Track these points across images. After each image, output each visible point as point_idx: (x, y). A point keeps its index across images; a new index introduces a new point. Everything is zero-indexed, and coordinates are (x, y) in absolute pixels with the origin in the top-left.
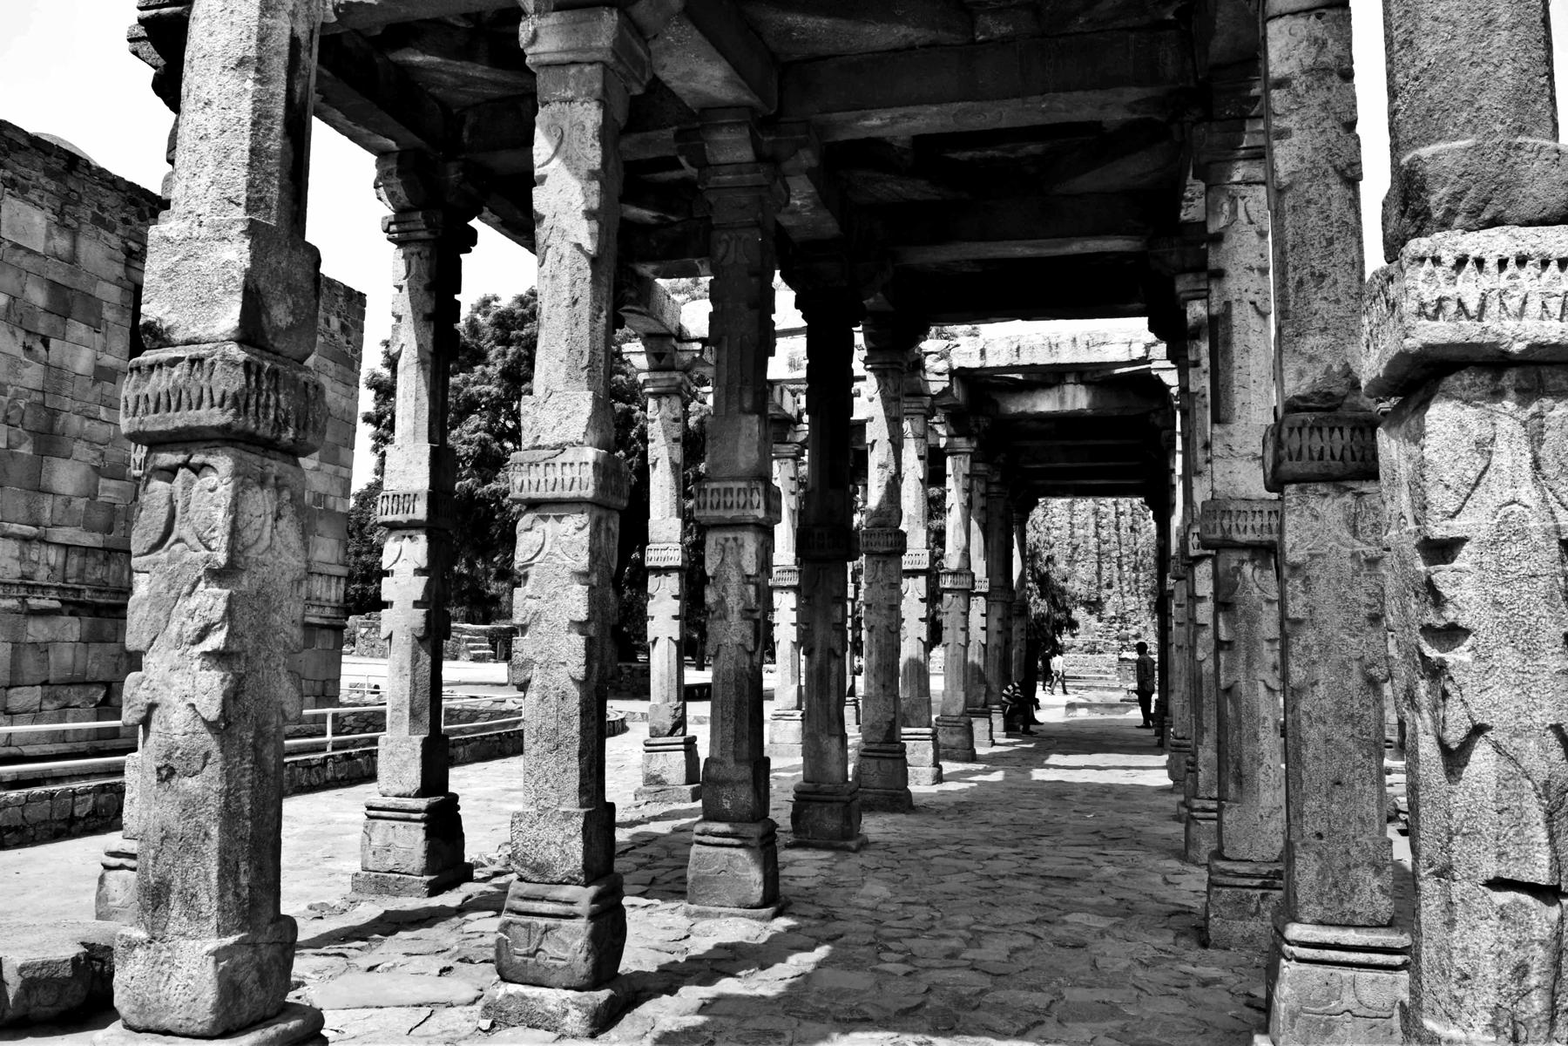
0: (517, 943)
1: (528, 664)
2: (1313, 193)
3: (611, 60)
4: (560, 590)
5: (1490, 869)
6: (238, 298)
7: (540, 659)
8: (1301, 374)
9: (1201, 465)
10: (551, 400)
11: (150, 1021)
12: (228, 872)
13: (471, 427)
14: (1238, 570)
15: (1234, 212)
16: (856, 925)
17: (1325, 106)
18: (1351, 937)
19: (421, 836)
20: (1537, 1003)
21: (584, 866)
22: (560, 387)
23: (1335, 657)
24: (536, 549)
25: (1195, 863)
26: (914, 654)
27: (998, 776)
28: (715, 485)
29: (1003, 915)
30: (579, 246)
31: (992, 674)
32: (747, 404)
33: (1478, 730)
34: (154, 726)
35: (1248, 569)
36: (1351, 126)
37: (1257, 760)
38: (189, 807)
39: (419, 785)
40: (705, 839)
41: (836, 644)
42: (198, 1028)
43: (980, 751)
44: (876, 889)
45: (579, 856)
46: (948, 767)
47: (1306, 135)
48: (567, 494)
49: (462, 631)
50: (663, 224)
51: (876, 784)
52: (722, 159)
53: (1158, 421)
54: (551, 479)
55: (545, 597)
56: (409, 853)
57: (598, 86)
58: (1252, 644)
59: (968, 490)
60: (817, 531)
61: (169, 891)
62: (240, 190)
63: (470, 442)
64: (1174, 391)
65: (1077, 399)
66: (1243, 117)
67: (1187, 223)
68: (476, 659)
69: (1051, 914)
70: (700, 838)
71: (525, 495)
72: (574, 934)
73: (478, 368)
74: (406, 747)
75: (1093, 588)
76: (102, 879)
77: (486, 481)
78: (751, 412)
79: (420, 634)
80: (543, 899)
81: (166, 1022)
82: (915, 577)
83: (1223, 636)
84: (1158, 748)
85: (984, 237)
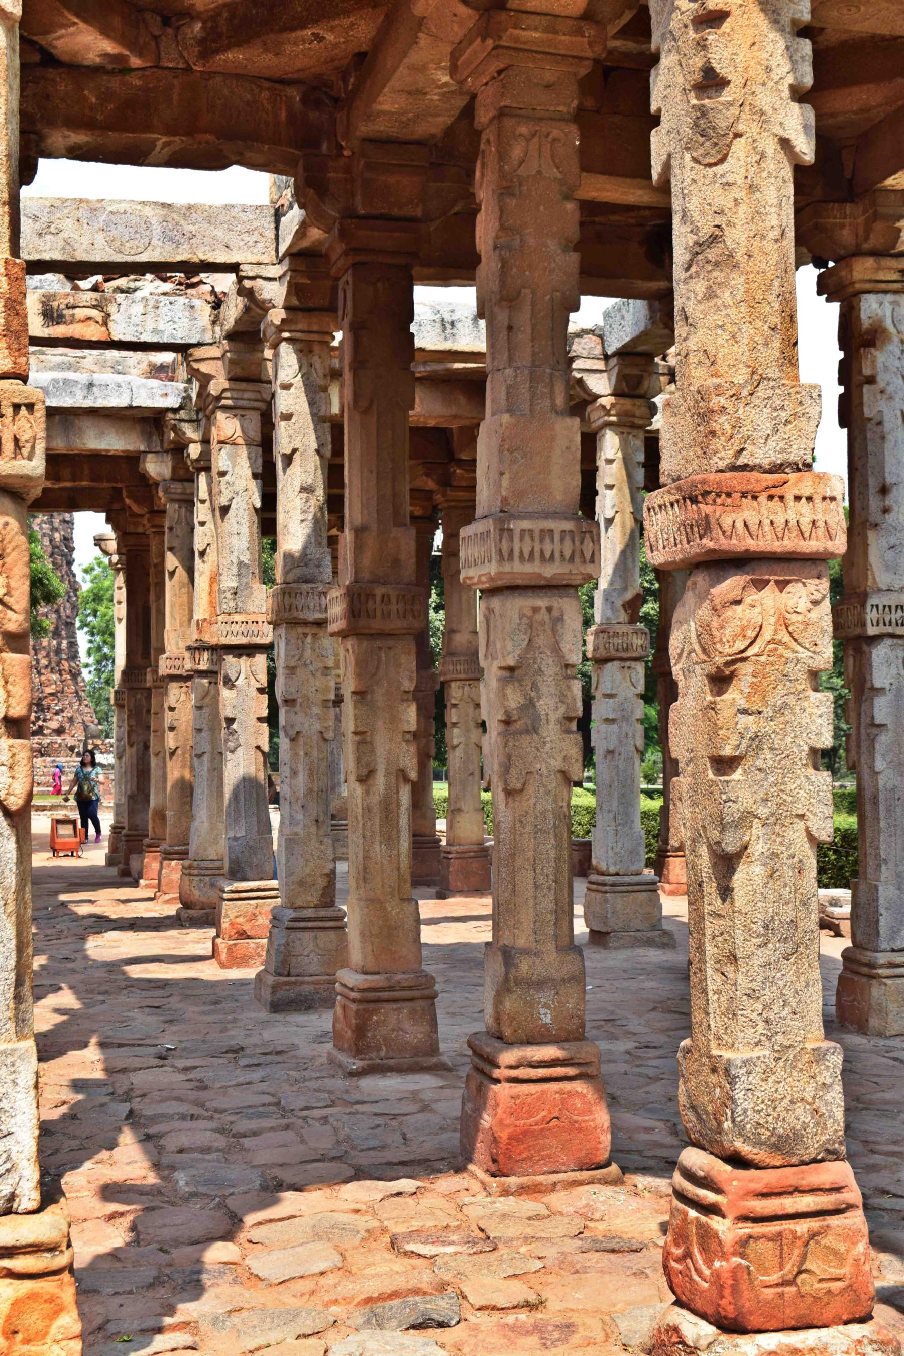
4: (791, 700)
7: (763, 811)
10: (761, 393)
21: (847, 1128)
22: (773, 372)
24: (751, 634)
25: (881, 1035)
26: (252, 771)
28: (526, 524)
30: (785, 143)
40: (522, 1073)
45: (839, 1115)
50: (116, 67)
51: (313, 969)
54: (780, 520)
55: (768, 712)
60: (379, 591)
70: (514, 1073)
80: (798, 1190)
82: (250, 655)
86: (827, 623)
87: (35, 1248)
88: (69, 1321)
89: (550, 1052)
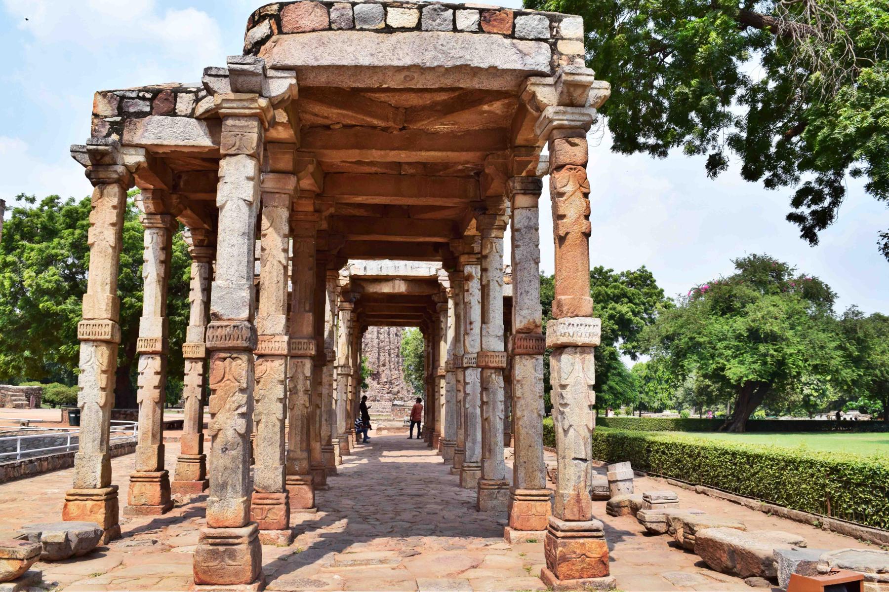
0: (257, 515)
1: (261, 413)
2: (526, 266)
3: (292, 193)
5: (573, 456)
6: (248, 307)
8: (521, 322)
9: (468, 331)
11: (220, 524)
12: (244, 479)
13: (51, 273)
14: (490, 376)
15: (492, 248)
16: (349, 513)
17: (530, 239)
18: (534, 492)
19: (159, 488)
20: (583, 484)
23: (530, 408)
27: (365, 461)
29: (404, 506)
30: (280, 262)
31: (352, 414)
32: (307, 308)
33: (571, 426)
34: (219, 436)
35: (493, 376)
36: (537, 246)
37: (496, 444)
38: (234, 459)
39: (156, 466)
41: (318, 402)
42: (240, 524)
43: (352, 451)
44: (347, 502)
46: (344, 458)
47: (524, 247)
48: (277, 352)
49: (8, 390)
52: (300, 210)
53: (436, 299)
56: (153, 496)
57: (287, 203)
58: (495, 402)
59: (348, 327)
61: (227, 484)
62: (245, 274)
63: (50, 282)
64: (448, 290)
65: (401, 288)
66: (496, 215)
67: (467, 236)
68: (17, 407)
69: (420, 506)
71: (260, 352)
72: (280, 510)
73: (56, 240)
74: (150, 450)
75: (375, 366)
76: (66, 506)
77: (58, 303)
78: (310, 311)
79: (157, 400)
81: (226, 524)
83: (485, 400)
84: (431, 446)
85: (385, 233)
86: (283, 370)
87: (97, 495)
88: (103, 510)
89: (297, 477)
